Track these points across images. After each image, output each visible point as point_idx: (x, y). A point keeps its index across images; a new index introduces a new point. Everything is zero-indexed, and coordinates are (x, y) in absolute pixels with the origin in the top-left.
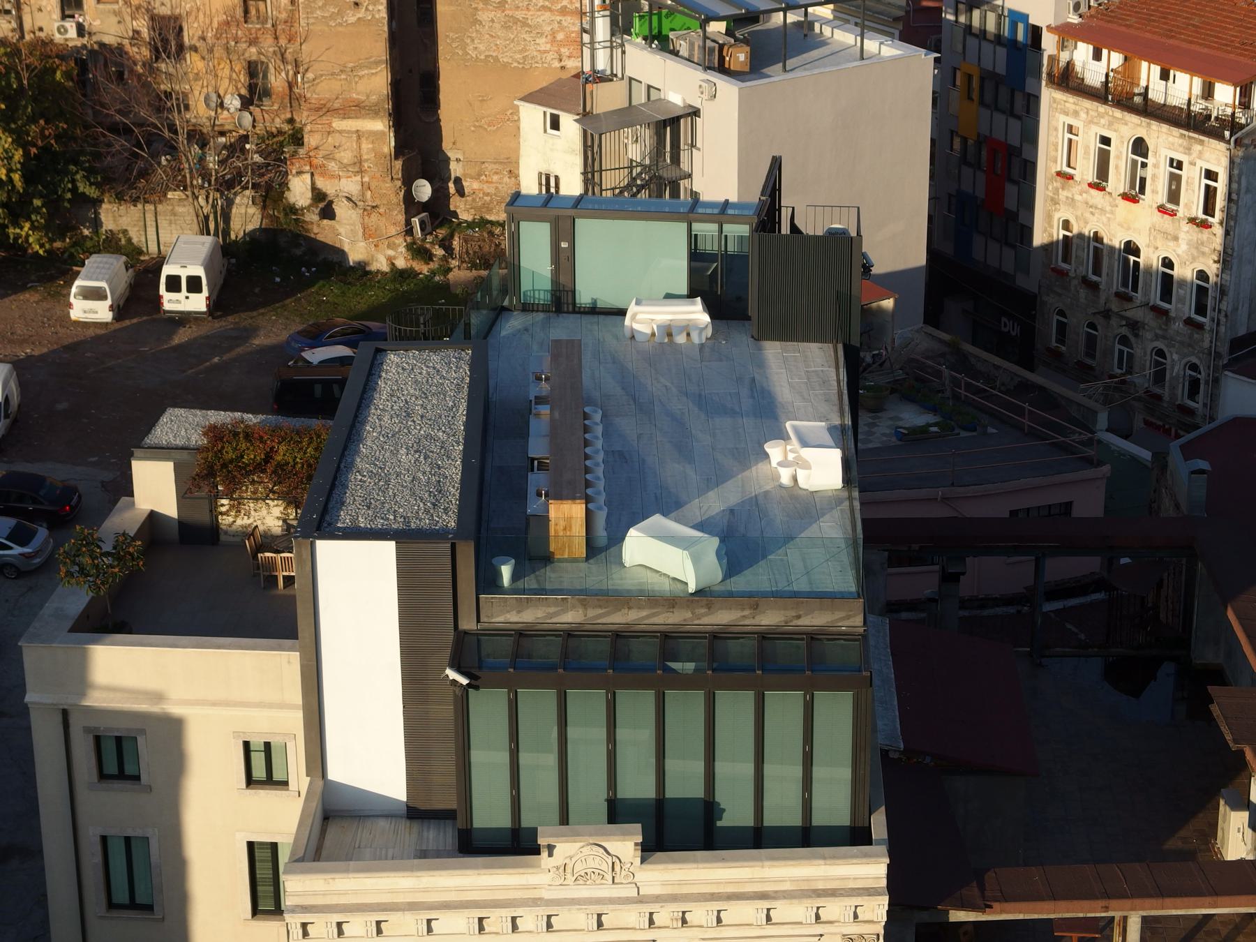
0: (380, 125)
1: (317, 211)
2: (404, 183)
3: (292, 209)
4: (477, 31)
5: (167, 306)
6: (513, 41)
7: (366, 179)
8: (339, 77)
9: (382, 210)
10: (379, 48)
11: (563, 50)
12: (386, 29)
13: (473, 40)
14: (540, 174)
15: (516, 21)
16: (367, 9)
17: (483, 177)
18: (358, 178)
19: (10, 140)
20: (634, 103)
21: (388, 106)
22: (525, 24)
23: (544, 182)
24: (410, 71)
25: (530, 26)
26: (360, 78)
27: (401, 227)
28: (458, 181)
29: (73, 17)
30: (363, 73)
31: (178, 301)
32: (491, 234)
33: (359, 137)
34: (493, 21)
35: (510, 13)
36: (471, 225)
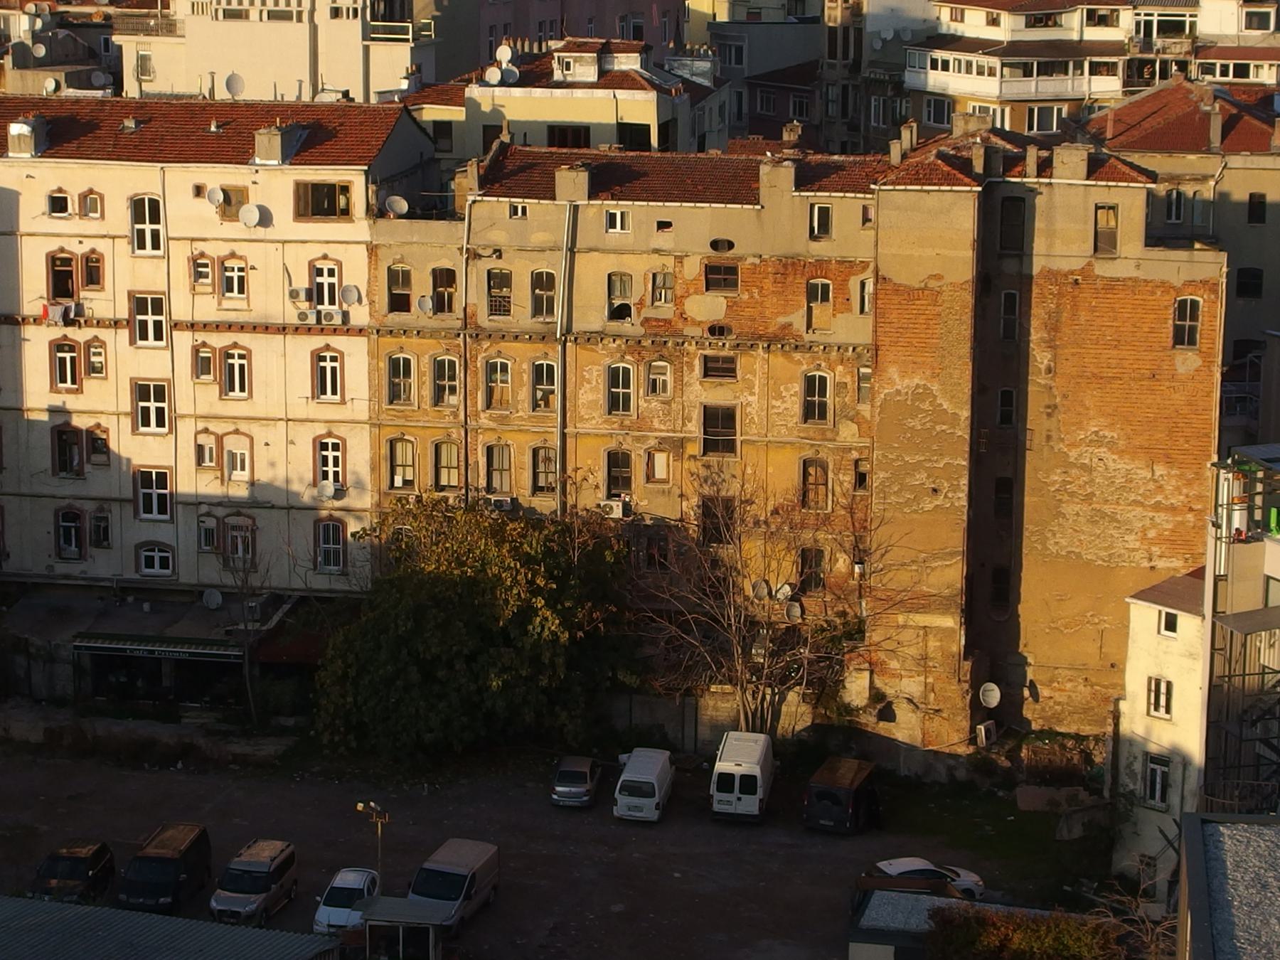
0: (950, 622)
1: (875, 712)
2: (971, 686)
3: (848, 709)
4: (1060, 525)
5: (716, 807)
6: (1098, 537)
7: (930, 680)
8: (909, 568)
9: (945, 715)
10: (956, 538)
11: (1154, 549)
12: (965, 518)
13: (1054, 535)
14: (1150, 679)
15: (1104, 515)
16: (946, 496)
17: (1055, 684)
18: (922, 678)
19: (557, 622)
20: (1271, 604)
21: (961, 600)
22: (1113, 519)
23: (1153, 687)
24: (983, 565)
25: (1118, 522)
26: (933, 569)
27: (965, 735)
28: (1033, 686)
29: (619, 496)
30: (936, 564)
31: (729, 803)
32: (1063, 747)
33: (926, 634)
34: (1078, 514)
35: (1098, 507)
36: (1042, 734)
